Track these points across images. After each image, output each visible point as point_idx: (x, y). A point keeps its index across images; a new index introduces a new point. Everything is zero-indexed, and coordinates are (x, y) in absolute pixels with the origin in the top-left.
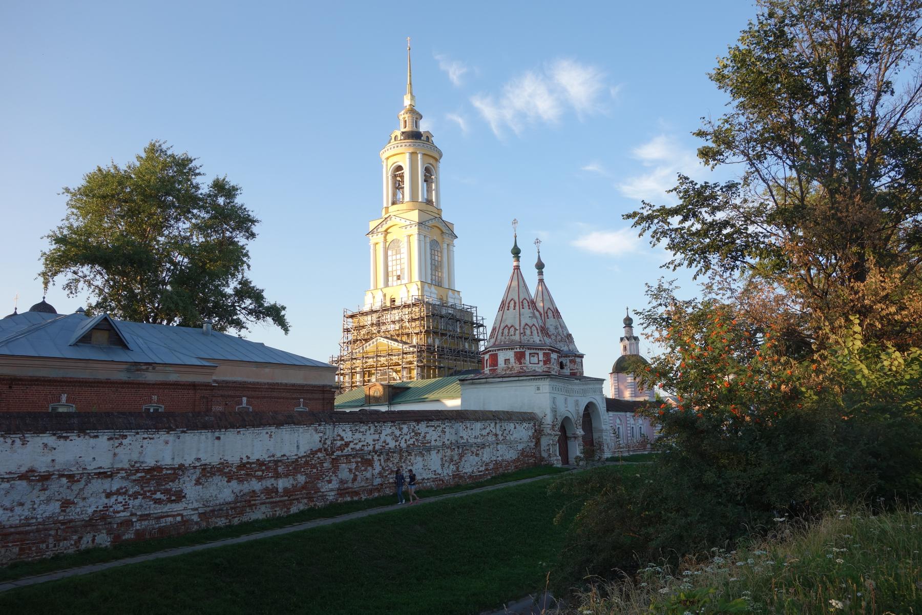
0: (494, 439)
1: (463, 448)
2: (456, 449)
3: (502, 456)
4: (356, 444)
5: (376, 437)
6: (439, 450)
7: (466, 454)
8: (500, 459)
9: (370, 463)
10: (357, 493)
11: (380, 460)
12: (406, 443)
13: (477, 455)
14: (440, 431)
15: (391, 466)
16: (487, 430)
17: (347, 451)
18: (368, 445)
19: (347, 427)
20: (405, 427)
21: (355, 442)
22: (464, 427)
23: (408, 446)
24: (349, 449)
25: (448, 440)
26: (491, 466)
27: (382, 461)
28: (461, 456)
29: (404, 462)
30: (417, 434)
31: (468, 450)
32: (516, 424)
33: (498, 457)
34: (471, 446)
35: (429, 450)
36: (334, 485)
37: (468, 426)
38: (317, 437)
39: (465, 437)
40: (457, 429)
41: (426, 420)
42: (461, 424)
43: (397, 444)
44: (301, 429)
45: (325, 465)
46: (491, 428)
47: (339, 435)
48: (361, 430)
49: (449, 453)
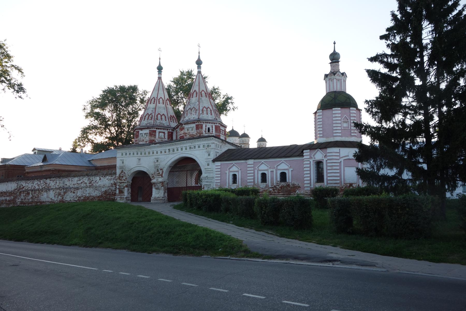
0: (85, 185)
1: (66, 189)
2: (63, 190)
3: (89, 194)
4: (26, 187)
5: (32, 185)
6: (54, 190)
7: (68, 192)
8: (88, 195)
9: (28, 194)
10: (25, 204)
11: (32, 193)
12: (42, 187)
13: (74, 193)
14: (55, 182)
15: (35, 195)
16: (81, 181)
17: (24, 189)
18: (29, 187)
19: (24, 182)
20: (42, 181)
21: (26, 186)
22: (68, 180)
23: (42, 188)
24: (24, 189)
25: (58, 186)
26: (82, 198)
27: (33, 193)
28: (65, 193)
29: (40, 194)
30: (46, 183)
31: (69, 190)
32: (101, 177)
33: (87, 194)
34: (71, 188)
35: (49, 190)
36: (20, 200)
37: (70, 179)
38: (16, 185)
39: (68, 185)
40: (64, 181)
41: (49, 178)
42: (66, 179)
43: (39, 187)
44: (13, 183)
45: (18, 194)
46: (84, 180)
47: (22, 184)
48: (28, 183)
49: (58, 191)
